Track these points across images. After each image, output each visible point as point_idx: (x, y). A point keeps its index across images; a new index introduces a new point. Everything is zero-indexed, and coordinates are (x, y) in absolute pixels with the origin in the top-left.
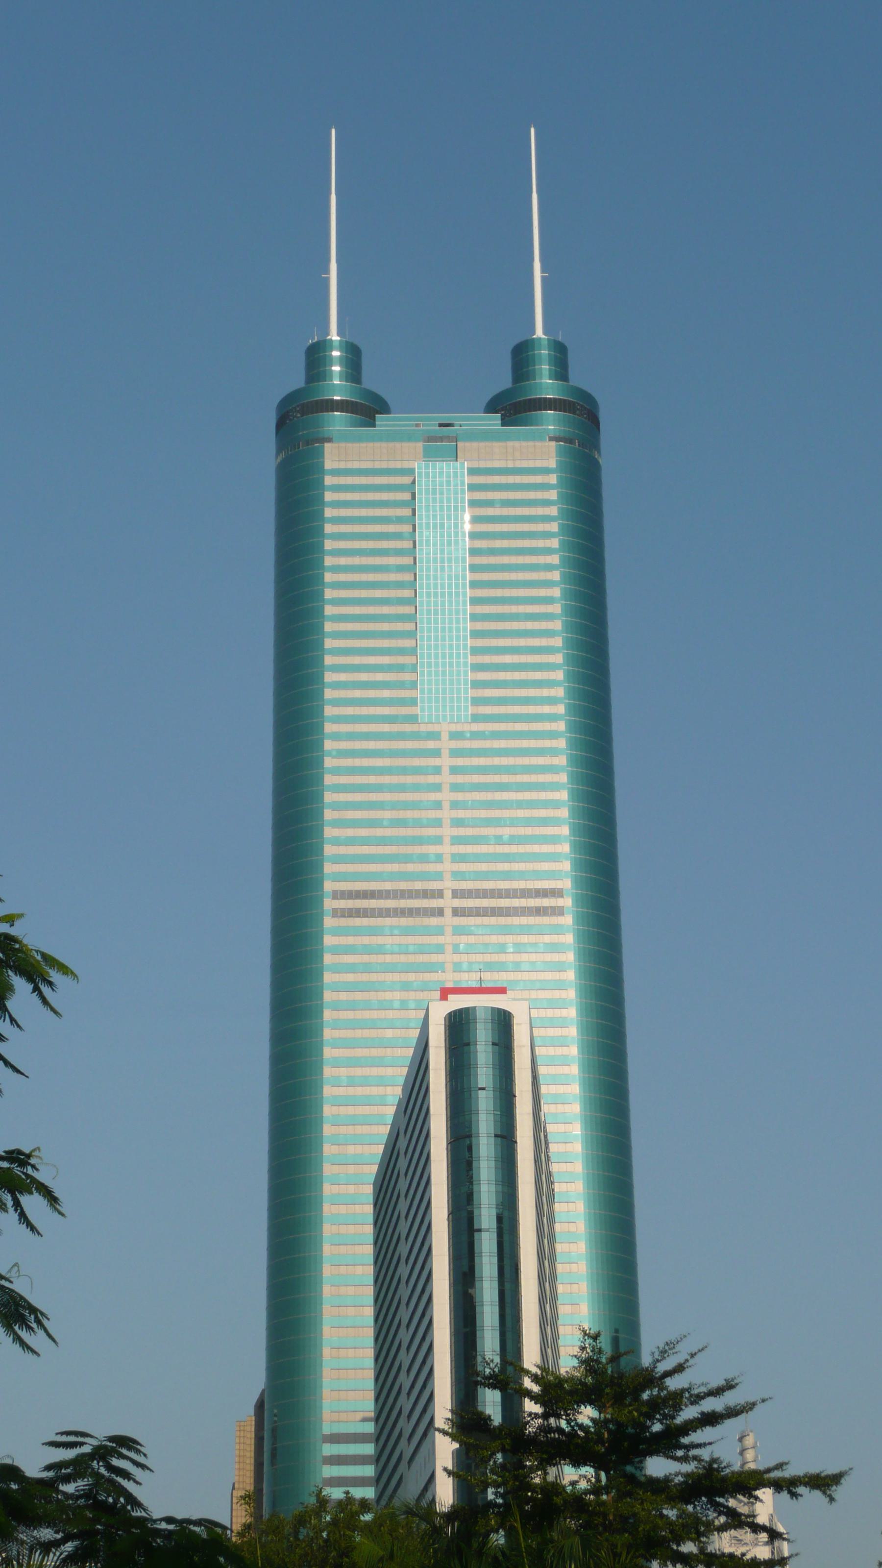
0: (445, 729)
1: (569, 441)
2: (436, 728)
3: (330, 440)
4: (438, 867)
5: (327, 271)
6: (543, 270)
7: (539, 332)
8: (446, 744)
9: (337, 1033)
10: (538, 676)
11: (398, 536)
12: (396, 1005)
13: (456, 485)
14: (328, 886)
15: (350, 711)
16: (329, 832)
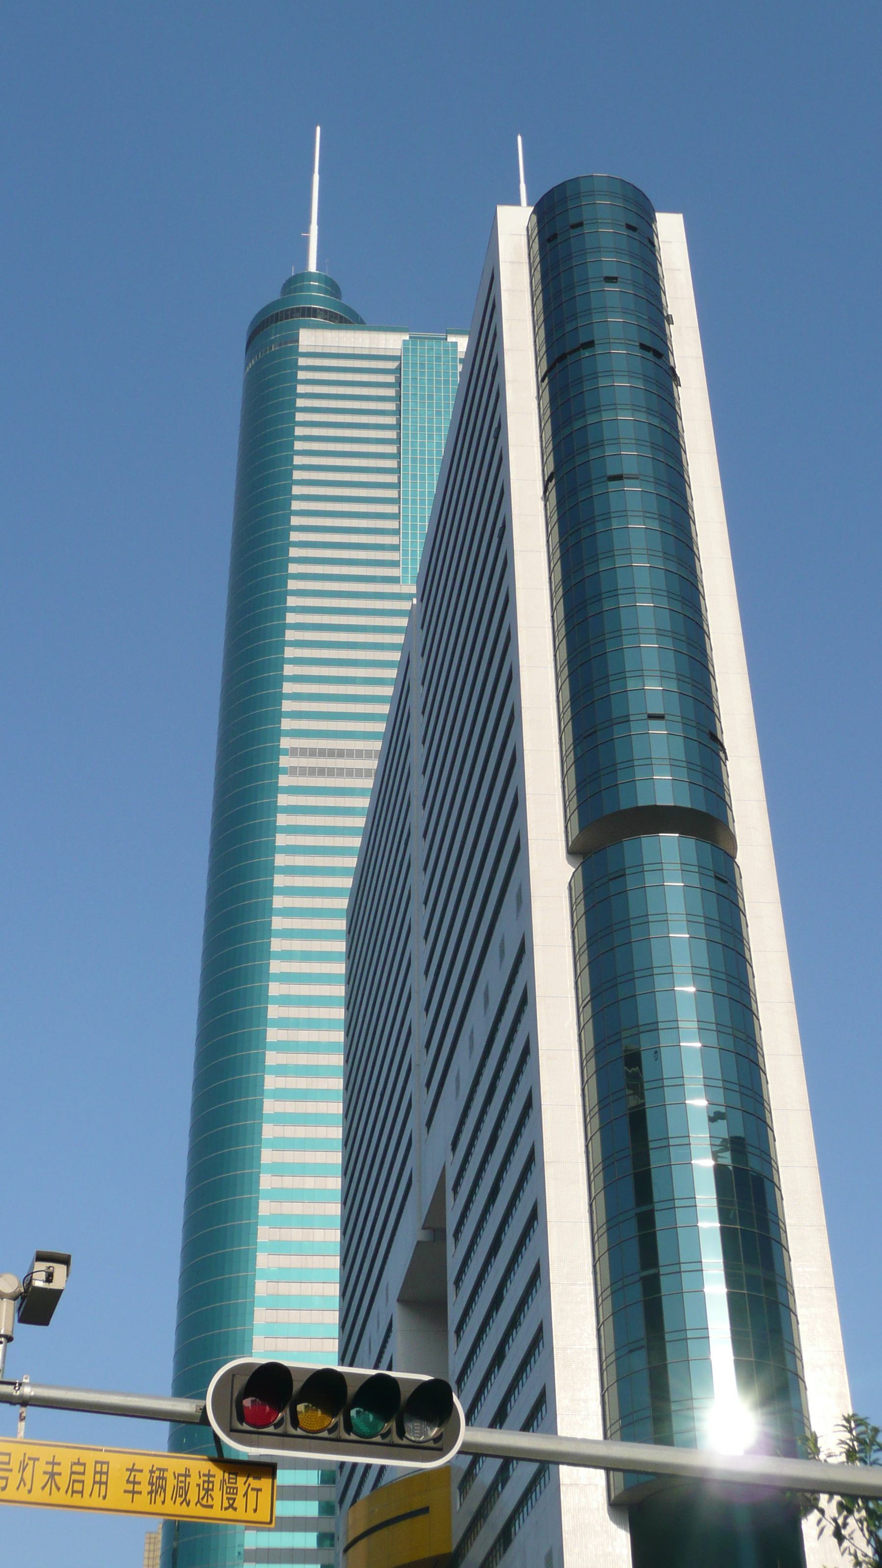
5: (307, 230)
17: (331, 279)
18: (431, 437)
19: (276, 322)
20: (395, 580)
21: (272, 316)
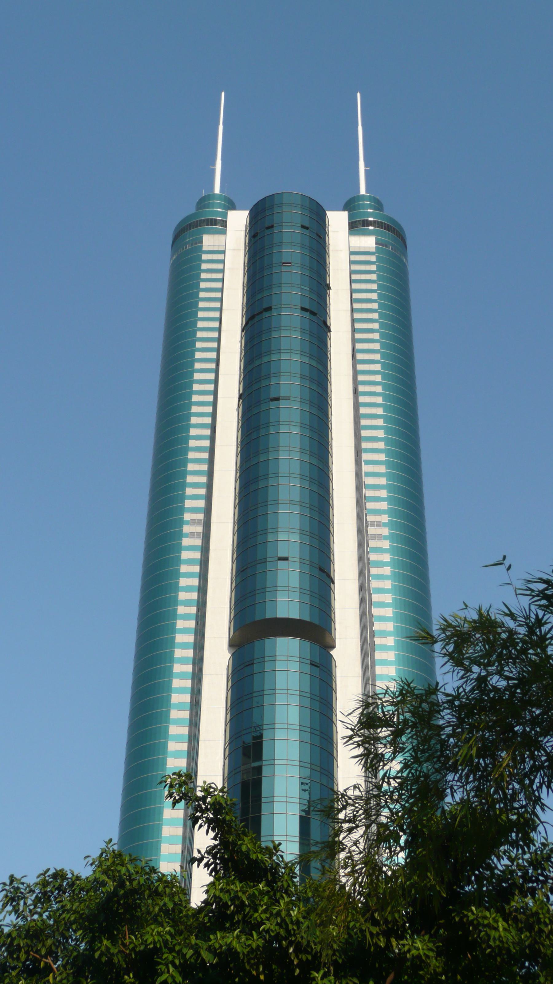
5: (214, 164)
6: (366, 165)
17: (229, 198)
19: (190, 229)
21: (187, 225)
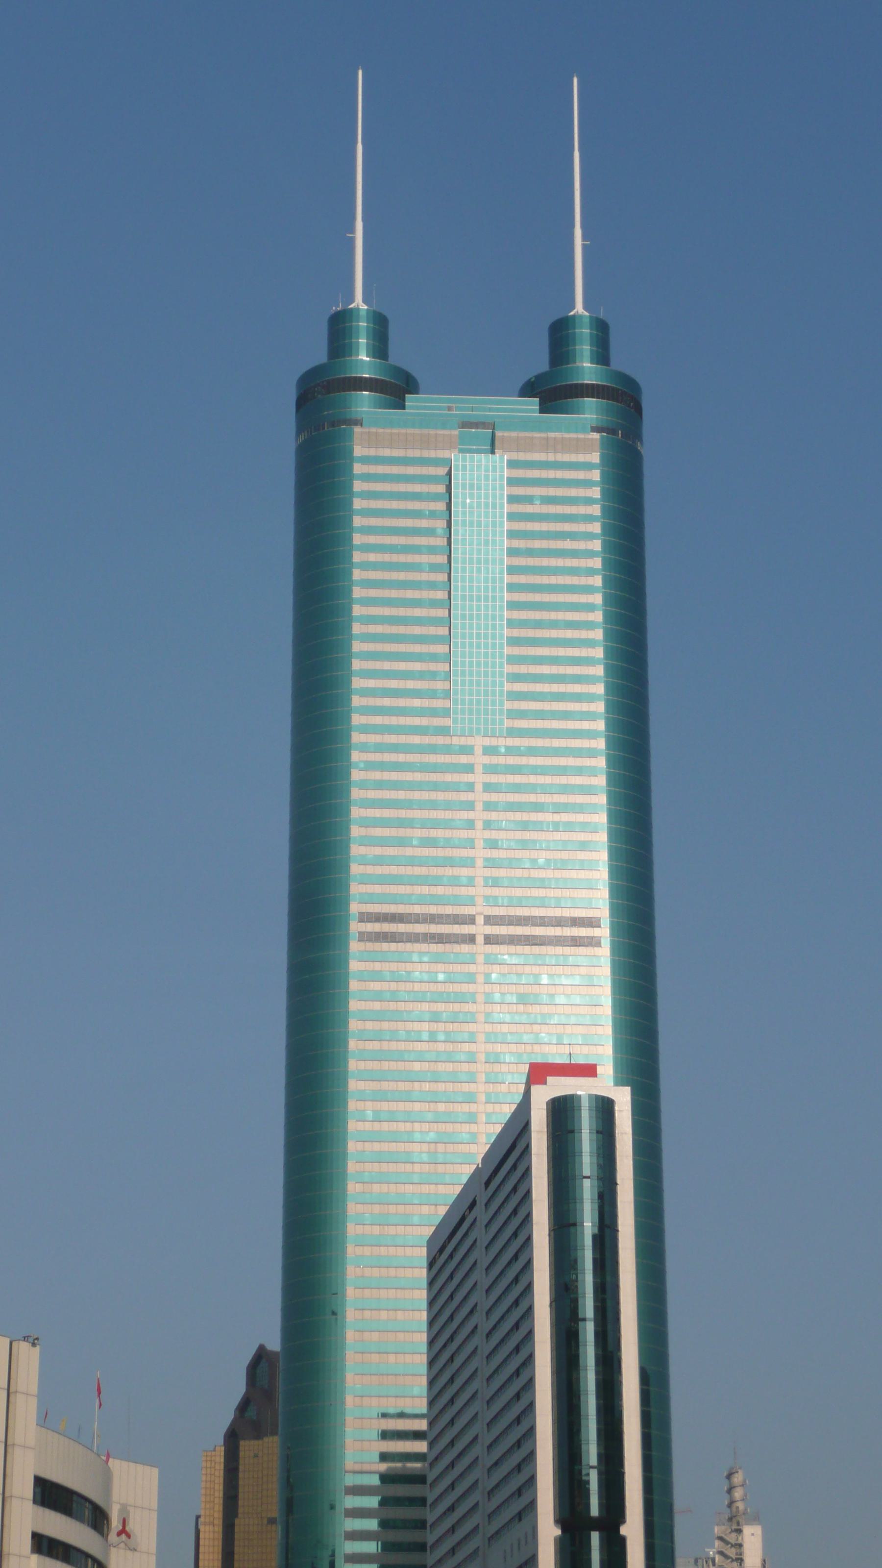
0: (479, 742)
1: (611, 431)
2: (470, 741)
3: (359, 422)
4: (471, 891)
5: (352, 230)
6: (584, 237)
7: (579, 308)
8: (480, 759)
9: (362, 1065)
10: (577, 688)
11: (430, 532)
12: (425, 1036)
13: (494, 480)
14: (355, 908)
15: (378, 720)
16: (356, 850)
18: (479, 571)
20: (444, 731)
